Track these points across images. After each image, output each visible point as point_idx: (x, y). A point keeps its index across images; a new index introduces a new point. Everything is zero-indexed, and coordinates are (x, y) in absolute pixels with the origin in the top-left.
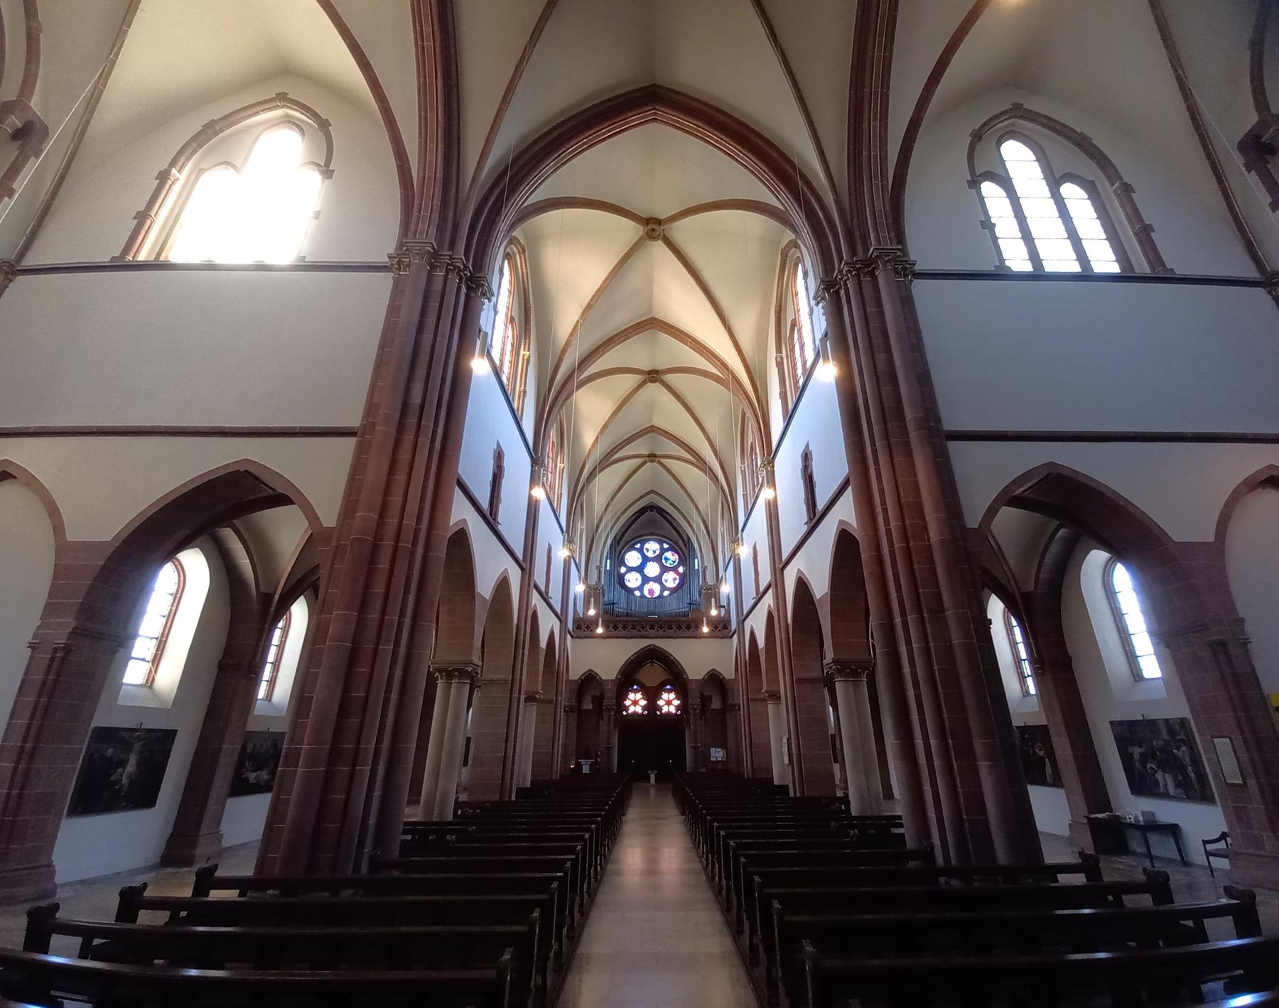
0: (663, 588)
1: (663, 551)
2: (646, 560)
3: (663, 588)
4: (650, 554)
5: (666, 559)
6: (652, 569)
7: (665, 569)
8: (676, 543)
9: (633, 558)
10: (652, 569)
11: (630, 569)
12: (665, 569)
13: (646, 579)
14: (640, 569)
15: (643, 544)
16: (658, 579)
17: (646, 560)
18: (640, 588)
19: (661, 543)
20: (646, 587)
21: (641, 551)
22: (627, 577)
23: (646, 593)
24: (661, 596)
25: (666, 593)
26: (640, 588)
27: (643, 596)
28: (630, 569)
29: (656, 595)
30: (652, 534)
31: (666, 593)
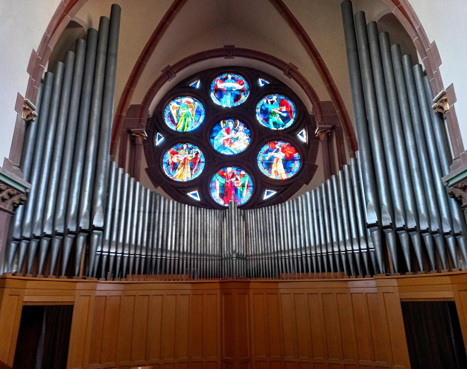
0: (260, 182)
1: (256, 94)
2: (214, 117)
3: (260, 182)
4: (227, 102)
5: (265, 112)
6: (233, 139)
7: (261, 137)
8: (291, 71)
9: (185, 114)
10: (233, 139)
11: (176, 139)
12: (260, 137)
13: (216, 162)
14: (201, 138)
15: (208, 76)
16: (246, 161)
17: (214, 117)
18: (202, 184)
19: (250, 75)
20: (218, 181)
21: (202, 96)
22: (168, 157)
23: (216, 195)
24: (255, 203)
25: (268, 195)
26: (202, 184)
27: (207, 203)
28: (176, 139)
29: (246, 196)
30: (229, 51)
31: (268, 195)
